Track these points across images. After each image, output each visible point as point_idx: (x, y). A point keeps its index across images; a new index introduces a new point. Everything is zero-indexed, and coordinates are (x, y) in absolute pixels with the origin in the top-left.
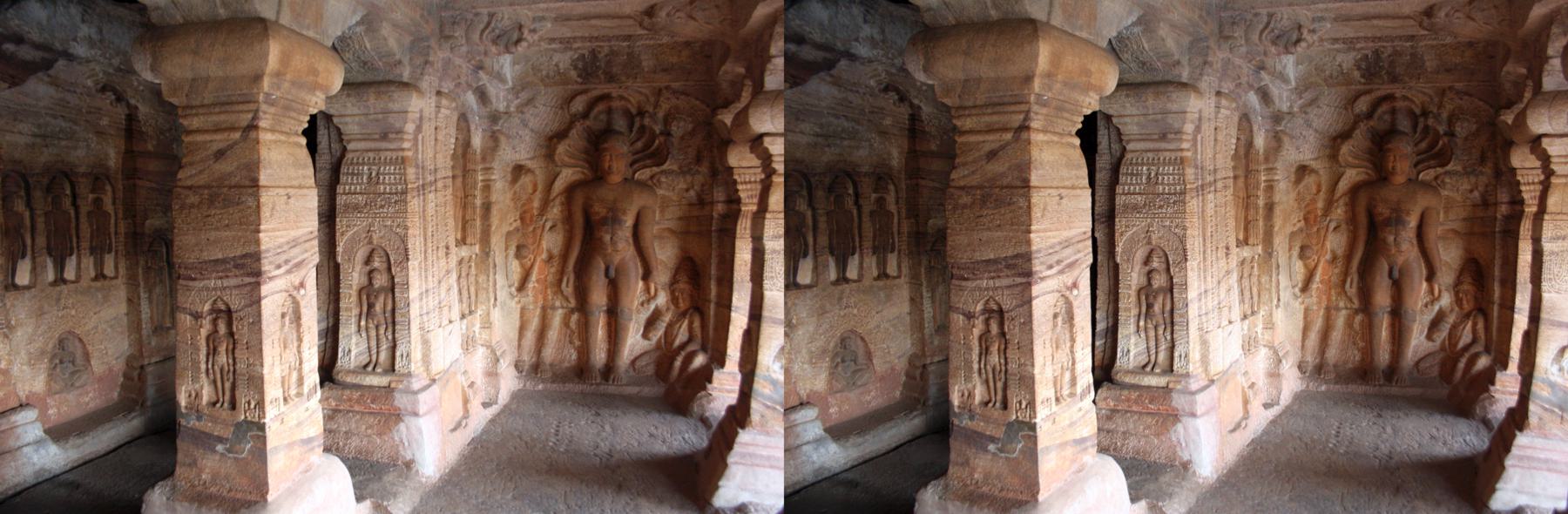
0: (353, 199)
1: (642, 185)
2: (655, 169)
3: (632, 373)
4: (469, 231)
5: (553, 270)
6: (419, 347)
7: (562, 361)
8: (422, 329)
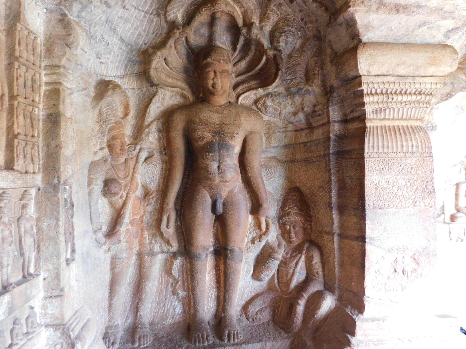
1: (248, 109)
2: (261, 92)
3: (245, 322)
5: (150, 208)
7: (164, 317)
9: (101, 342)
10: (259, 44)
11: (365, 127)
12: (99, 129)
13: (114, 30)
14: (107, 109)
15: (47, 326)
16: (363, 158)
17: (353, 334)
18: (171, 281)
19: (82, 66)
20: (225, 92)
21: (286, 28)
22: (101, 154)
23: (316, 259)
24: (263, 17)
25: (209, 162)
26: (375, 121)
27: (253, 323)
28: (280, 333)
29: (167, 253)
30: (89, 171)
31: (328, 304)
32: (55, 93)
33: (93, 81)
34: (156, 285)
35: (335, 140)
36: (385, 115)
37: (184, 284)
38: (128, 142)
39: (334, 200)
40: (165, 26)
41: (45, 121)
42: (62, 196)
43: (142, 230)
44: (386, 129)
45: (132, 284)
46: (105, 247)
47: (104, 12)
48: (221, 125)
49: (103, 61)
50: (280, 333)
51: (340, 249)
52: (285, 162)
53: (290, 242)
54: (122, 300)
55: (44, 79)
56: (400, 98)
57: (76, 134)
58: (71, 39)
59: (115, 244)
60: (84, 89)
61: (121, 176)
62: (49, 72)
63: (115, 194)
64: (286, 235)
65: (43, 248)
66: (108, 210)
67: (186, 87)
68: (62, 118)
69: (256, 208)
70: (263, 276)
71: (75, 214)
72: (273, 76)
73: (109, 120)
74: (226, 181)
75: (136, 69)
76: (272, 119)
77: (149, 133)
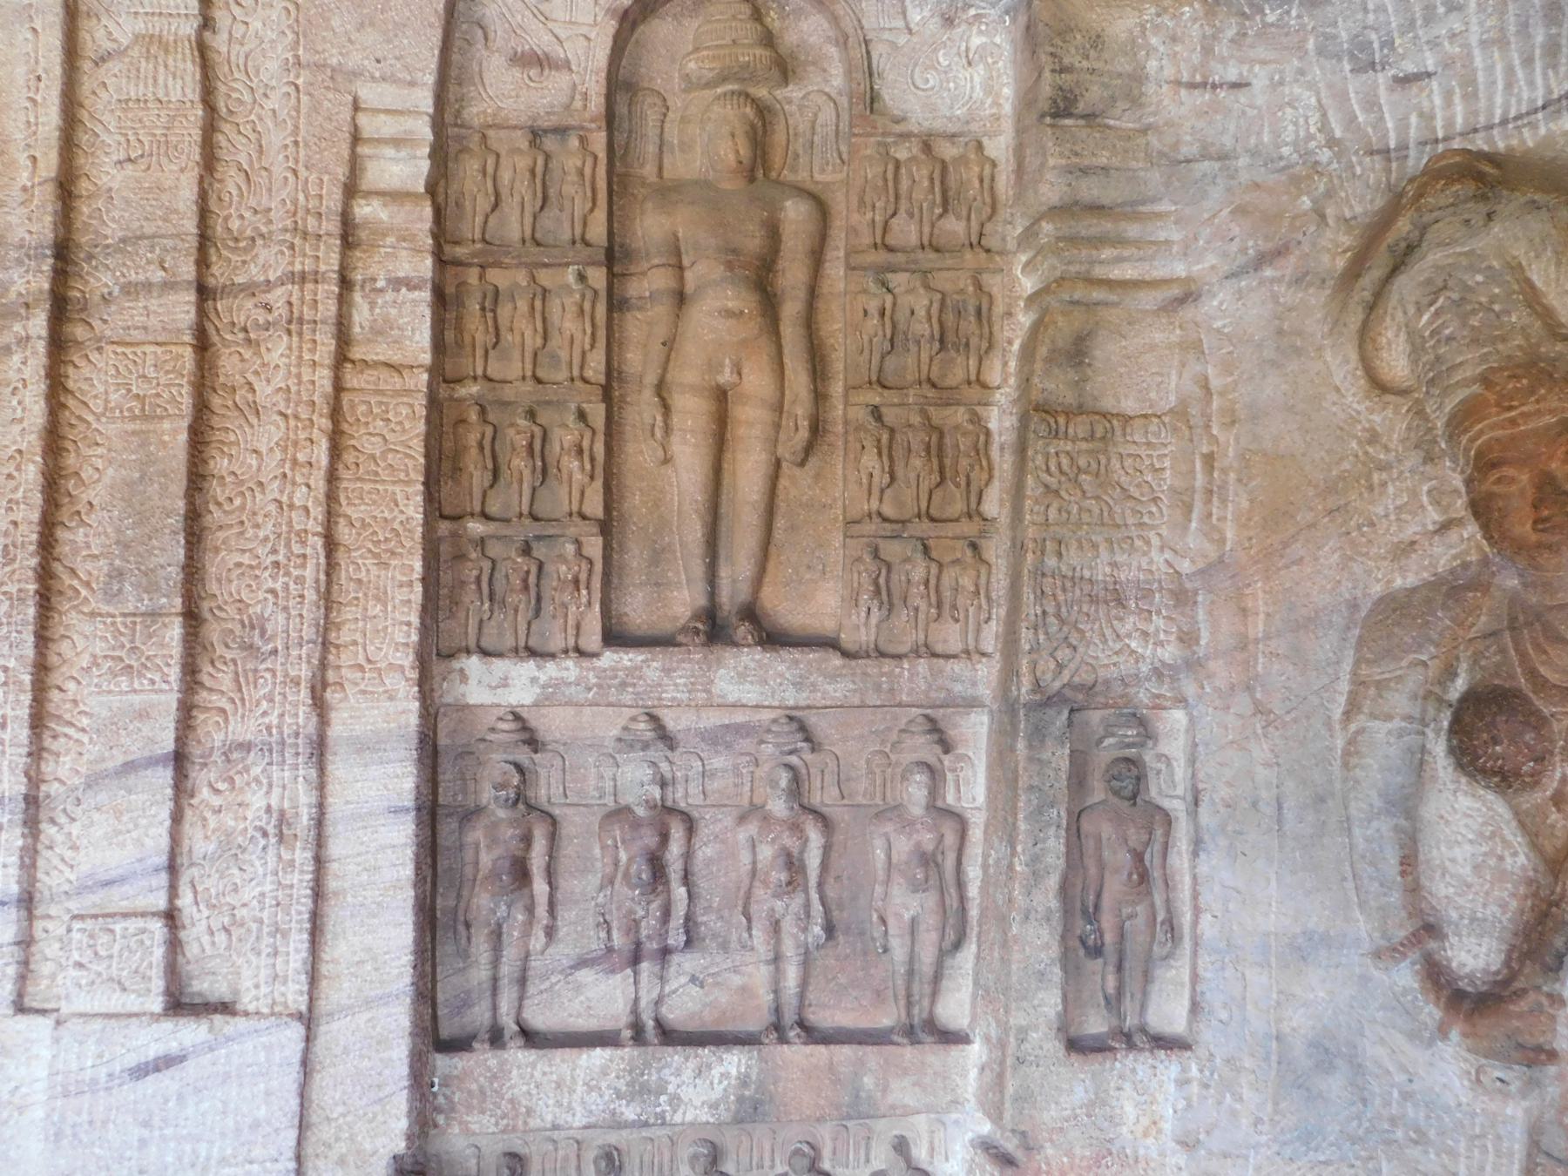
12: (1409, 428)
14: (1437, 314)
19: (1223, 157)
55: (1028, 285)
57: (1232, 476)
60: (1261, 260)
66: (1522, 859)
73: (1453, 368)
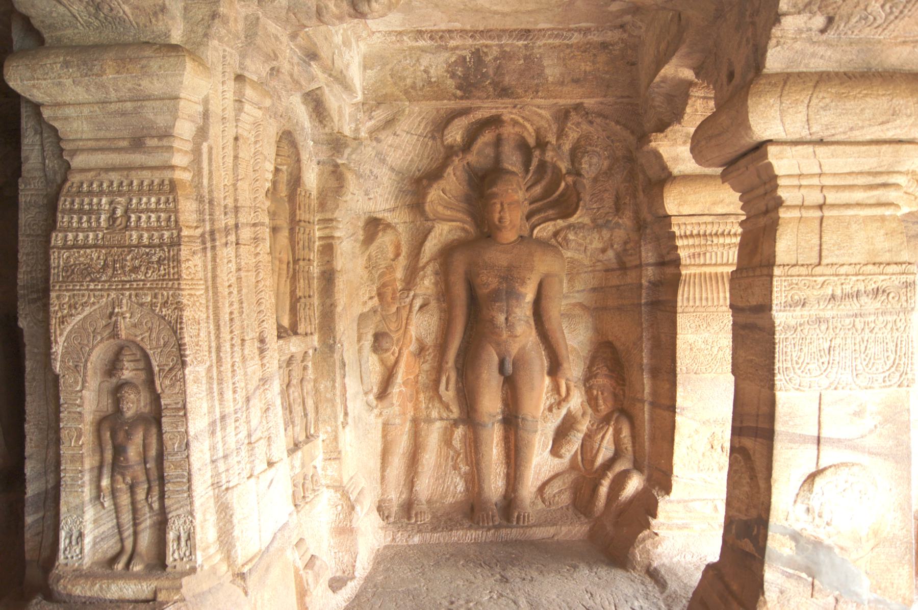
0: (81, 257)
1: (543, 244)
2: (561, 223)
3: (540, 505)
4: (301, 314)
5: (426, 367)
6: (212, 518)
8: (216, 485)
9: (376, 513)
10: (556, 169)
11: (680, 275)
13: (383, 161)
15: (328, 487)
16: (676, 312)
17: (654, 516)
18: (452, 453)
20: (514, 226)
21: (589, 148)
22: (370, 304)
23: (626, 432)
24: (561, 134)
25: (494, 314)
26: (692, 268)
27: (549, 507)
28: (579, 518)
29: (447, 419)
30: (359, 324)
31: (634, 484)
32: (328, 249)
33: (361, 224)
34: (434, 458)
35: (648, 288)
36: (705, 260)
37: (466, 457)
38: (400, 288)
39: (645, 361)
40: (442, 150)
41: (319, 279)
42: (337, 356)
43: (417, 393)
44: (705, 278)
45: (407, 455)
46: (376, 411)
47: (374, 148)
48: (510, 268)
49: (372, 196)
50: (579, 518)
51: (652, 420)
52: (595, 309)
53: (598, 411)
54: (395, 472)
55: (318, 234)
56: (721, 240)
58: (344, 189)
59: (387, 407)
61: (392, 329)
62: (321, 226)
63: (387, 350)
64: (593, 402)
65: (321, 410)
67: (469, 219)
68: (337, 275)
69: (555, 368)
70: (563, 451)
71: (347, 374)
72: (574, 206)
74: (516, 336)
75: (408, 199)
76: (576, 256)
77: (425, 276)
